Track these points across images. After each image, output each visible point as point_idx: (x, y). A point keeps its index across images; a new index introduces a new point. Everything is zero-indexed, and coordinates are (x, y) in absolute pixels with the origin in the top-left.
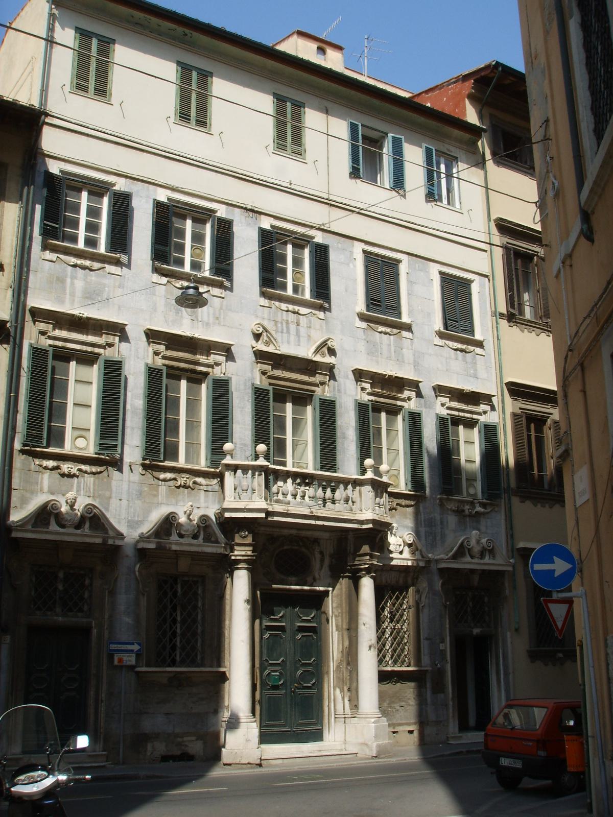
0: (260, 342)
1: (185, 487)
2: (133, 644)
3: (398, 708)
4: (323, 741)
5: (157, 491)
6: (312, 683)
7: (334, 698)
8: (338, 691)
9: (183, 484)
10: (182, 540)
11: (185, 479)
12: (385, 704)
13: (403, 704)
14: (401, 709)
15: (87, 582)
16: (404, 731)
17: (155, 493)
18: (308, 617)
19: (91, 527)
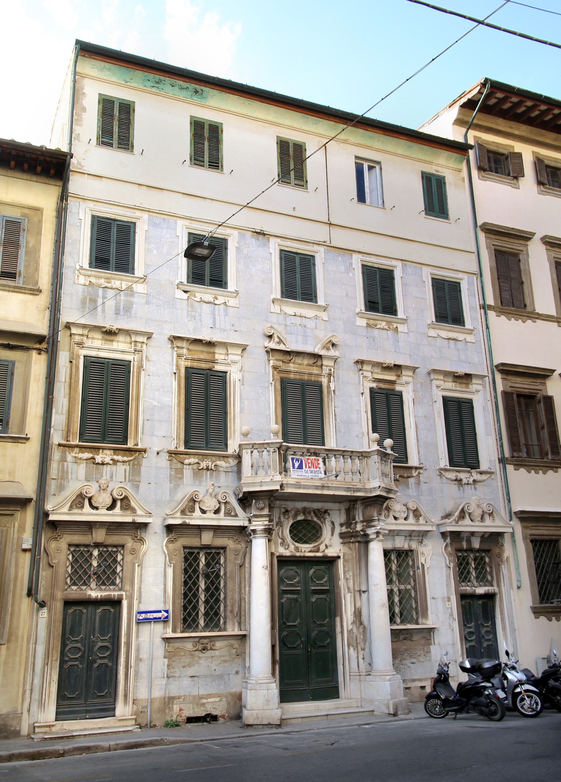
0: (272, 342)
1: (207, 469)
2: (160, 612)
3: (409, 664)
4: (338, 697)
5: (182, 473)
6: (327, 642)
7: (347, 657)
8: (352, 649)
9: (205, 467)
10: (204, 515)
11: (207, 462)
12: (397, 661)
13: (414, 660)
14: (412, 665)
15: (119, 558)
16: (415, 687)
17: (180, 476)
18: (321, 580)
19: (122, 508)
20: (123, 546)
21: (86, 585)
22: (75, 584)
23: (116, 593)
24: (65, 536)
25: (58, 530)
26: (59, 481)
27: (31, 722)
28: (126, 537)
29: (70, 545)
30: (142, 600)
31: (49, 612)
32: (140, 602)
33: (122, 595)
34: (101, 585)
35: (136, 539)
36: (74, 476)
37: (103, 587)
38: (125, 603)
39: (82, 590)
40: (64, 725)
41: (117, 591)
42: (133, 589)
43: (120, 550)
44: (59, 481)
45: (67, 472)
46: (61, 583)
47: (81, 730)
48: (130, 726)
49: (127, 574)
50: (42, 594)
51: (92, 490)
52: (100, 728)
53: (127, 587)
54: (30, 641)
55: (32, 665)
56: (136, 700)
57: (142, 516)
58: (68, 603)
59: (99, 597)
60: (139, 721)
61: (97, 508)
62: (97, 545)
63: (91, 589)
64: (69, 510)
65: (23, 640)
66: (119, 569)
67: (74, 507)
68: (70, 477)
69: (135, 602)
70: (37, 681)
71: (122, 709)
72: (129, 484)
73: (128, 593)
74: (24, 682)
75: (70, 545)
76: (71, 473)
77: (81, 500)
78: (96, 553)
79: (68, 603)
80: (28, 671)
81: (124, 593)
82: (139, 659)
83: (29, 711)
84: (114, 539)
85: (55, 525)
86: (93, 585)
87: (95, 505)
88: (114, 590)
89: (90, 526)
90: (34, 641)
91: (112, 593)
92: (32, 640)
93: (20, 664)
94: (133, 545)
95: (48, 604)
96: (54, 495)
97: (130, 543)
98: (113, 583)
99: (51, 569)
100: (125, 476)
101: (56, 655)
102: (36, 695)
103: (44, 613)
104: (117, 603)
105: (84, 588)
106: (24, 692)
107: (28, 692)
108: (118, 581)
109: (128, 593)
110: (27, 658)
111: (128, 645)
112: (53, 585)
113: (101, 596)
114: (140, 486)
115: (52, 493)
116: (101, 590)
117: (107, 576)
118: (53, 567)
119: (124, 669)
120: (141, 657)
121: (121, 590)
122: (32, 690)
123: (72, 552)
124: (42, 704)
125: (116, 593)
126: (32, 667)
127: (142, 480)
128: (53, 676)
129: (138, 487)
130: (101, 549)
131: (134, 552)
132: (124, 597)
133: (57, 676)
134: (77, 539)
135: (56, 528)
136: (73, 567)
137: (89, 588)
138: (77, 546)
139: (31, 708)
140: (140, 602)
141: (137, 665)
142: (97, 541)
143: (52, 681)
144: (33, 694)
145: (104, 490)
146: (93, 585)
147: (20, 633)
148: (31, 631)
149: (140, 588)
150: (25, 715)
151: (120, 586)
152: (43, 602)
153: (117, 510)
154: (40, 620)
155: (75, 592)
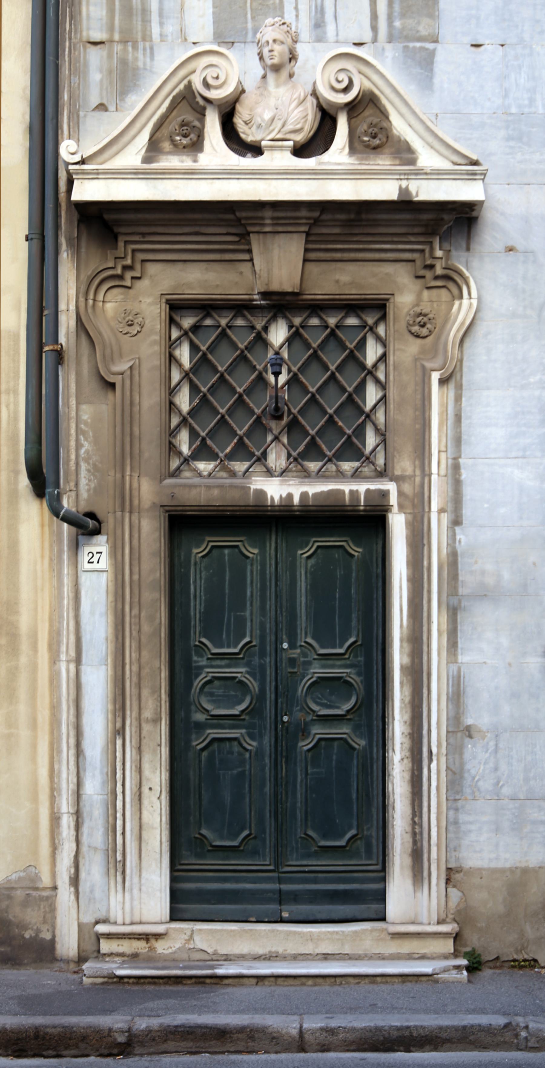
19: (356, 145)
20: (380, 307)
21: (249, 455)
22: (202, 451)
23: (362, 488)
24: (152, 269)
25: (121, 244)
26: (118, 48)
27: (88, 918)
28: (388, 268)
29: (176, 307)
30: (467, 512)
31: (115, 552)
32: (457, 522)
33: (385, 494)
34: (304, 456)
35: (429, 274)
36: (171, 28)
37: (313, 466)
38: (398, 524)
39: (233, 474)
40: (197, 938)
41: (366, 478)
42: (426, 474)
43: (370, 321)
44: (118, 48)
46: (151, 449)
47: (257, 958)
48: (436, 960)
49: (401, 416)
50: (80, 488)
51: (235, 70)
52: (326, 957)
53: (404, 465)
54: (58, 652)
55: (72, 733)
56: (459, 870)
57: (438, 174)
58: (183, 524)
59: (296, 500)
60: (474, 940)
61: (256, 150)
62: (280, 304)
63: (269, 473)
64: (146, 160)
65: (35, 648)
66: (372, 394)
67: (167, 145)
68: (155, 30)
69: (437, 524)
70: (93, 787)
71: (401, 895)
73: (407, 488)
74: (52, 789)
75: (176, 307)
76: (161, 15)
77: (189, 117)
78: (278, 334)
79: (183, 524)
80: (60, 752)
81: (391, 487)
82: (461, 731)
83: (75, 881)
84: (345, 278)
85: (103, 222)
86: (277, 458)
87: (248, 134)
88: (356, 475)
89: (235, 223)
90: (73, 653)
91: (346, 487)
92: (64, 648)
93: (34, 725)
94: (419, 295)
95: (109, 523)
96: (102, 107)
97: (407, 296)
98: (352, 449)
99: (110, 395)
100: (374, 16)
101: (154, 703)
102: (95, 834)
103: (98, 555)
104: (369, 523)
105: (240, 466)
106: (55, 819)
107: (67, 822)
108: (371, 440)
109: (407, 488)
110: (55, 708)
111: (417, 675)
112: (124, 451)
113: (304, 495)
114: (439, 57)
116: (306, 475)
117: (331, 423)
118: (112, 386)
119: (408, 764)
120: (469, 721)
121: (382, 474)
122: (78, 815)
123: (186, 333)
124: (116, 865)
125: (362, 488)
126: (72, 741)
127: (446, 31)
128: (147, 772)
129: (427, 62)
130: (297, 321)
131: (423, 326)
132: (393, 500)
133: (165, 776)
134: (200, 279)
135: (115, 237)
136: (194, 389)
137: (258, 468)
138: (206, 307)
139: (83, 875)
140: (457, 522)
141: (455, 750)
142: (275, 287)
143: (145, 790)
144: (85, 830)
145: (276, 69)
146: (277, 458)
147: (24, 621)
148: (61, 617)
149: (456, 468)
150: (65, 895)
151: (380, 461)
152: (91, 515)
153: (338, 153)
154: (85, 579)
155: (204, 483)
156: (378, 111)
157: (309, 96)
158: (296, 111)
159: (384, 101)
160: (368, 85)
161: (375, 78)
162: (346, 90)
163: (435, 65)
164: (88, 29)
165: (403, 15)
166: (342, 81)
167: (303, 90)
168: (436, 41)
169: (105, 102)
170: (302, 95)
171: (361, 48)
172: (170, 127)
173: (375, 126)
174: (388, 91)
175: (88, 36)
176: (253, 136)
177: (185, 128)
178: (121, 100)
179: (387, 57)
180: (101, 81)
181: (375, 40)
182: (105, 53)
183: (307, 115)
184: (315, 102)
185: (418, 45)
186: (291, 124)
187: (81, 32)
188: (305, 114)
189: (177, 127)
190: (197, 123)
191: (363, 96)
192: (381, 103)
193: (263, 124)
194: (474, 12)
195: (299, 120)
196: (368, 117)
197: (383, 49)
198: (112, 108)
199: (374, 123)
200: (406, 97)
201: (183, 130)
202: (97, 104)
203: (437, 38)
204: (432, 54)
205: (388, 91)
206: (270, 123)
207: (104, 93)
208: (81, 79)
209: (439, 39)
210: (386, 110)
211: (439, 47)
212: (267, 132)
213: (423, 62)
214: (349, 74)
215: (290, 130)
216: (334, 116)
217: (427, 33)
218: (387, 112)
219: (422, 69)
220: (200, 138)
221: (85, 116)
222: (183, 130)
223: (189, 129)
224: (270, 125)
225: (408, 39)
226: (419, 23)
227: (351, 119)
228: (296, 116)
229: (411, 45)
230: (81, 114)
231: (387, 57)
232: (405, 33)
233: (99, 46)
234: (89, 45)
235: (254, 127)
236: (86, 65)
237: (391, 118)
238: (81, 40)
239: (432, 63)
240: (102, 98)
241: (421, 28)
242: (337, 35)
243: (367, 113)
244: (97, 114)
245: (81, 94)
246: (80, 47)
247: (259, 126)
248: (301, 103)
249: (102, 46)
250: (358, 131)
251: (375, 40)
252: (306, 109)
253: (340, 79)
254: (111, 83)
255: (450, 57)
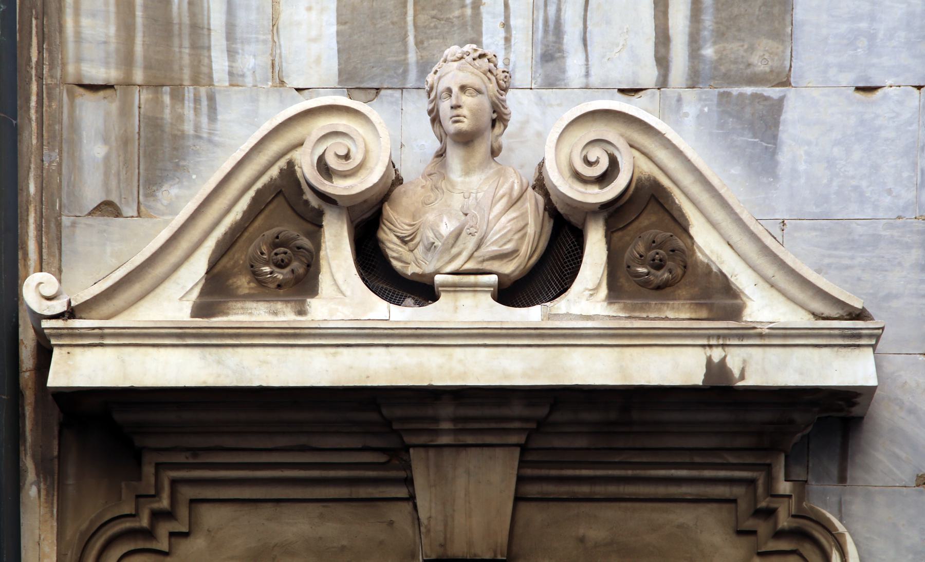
36: (251, 61)
45: (198, 30)
68: (219, 64)
72: (694, 104)
96: (108, 209)
114: (790, 114)
115: (92, 195)
127: (806, 62)
129: (765, 123)
156: (667, 219)
157: (530, 189)
158: (504, 219)
159: (680, 199)
160: (647, 168)
161: (662, 155)
162: (603, 180)
163: (781, 128)
164: (79, 60)
165: (720, 35)
166: (597, 162)
167: (516, 177)
168: (786, 83)
169: (114, 198)
170: (517, 187)
171: (635, 98)
172: (251, 249)
173: (660, 246)
174: (687, 180)
175: (79, 73)
176: (418, 265)
177: (282, 249)
178: (146, 196)
179: (686, 115)
180: (107, 158)
181: (663, 83)
182: (114, 107)
183: (527, 225)
184: (541, 200)
185: (749, 90)
186: (493, 244)
187: (64, 65)
188: (522, 224)
189: (264, 249)
190: (305, 242)
191: (637, 188)
192: (673, 202)
193: (438, 243)
194: (864, 25)
195: (509, 237)
196: (647, 228)
197: (679, 100)
198: (129, 210)
199: (658, 240)
200: (722, 191)
201: (276, 254)
202: (99, 202)
203: (788, 76)
204: (777, 107)
205: (687, 180)
206: (451, 241)
207: (113, 183)
208: (65, 155)
209: (792, 80)
210: (683, 215)
211: (790, 93)
212: (447, 258)
213: (757, 125)
214: (611, 150)
215: (493, 254)
216: (580, 227)
217: (767, 69)
218: (686, 220)
219: (755, 136)
220: (312, 269)
221: (74, 225)
222: (276, 254)
223: (289, 252)
224: (453, 246)
225: (730, 79)
226: (752, 49)
227: (612, 232)
228: (504, 227)
229: (735, 91)
230: (66, 221)
231: (686, 115)
232: (723, 69)
233: (101, 94)
234: (81, 91)
235: (421, 248)
236: (74, 127)
237: (693, 231)
238: (63, 81)
239: (776, 124)
240: (108, 191)
241: (755, 59)
242: (587, 74)
243: (644, 221)
244: (99, 222)
245: (64, 184)
246: (61, 93)
247: (431, 247)
248: (513, 203)
249: (109, 92)
250: (627, 255)
251: (663, 83)
252: (524, 215)
253: (592, 158)
254: (126, 163)
255: (812, 115)
